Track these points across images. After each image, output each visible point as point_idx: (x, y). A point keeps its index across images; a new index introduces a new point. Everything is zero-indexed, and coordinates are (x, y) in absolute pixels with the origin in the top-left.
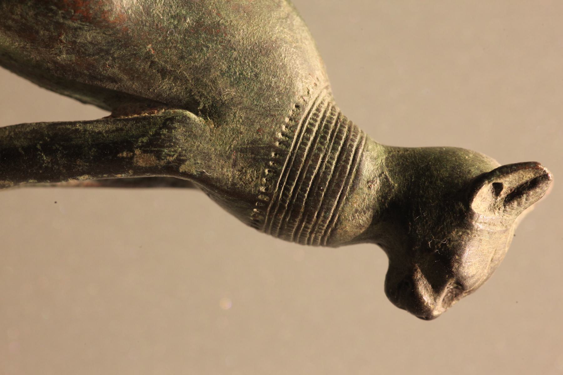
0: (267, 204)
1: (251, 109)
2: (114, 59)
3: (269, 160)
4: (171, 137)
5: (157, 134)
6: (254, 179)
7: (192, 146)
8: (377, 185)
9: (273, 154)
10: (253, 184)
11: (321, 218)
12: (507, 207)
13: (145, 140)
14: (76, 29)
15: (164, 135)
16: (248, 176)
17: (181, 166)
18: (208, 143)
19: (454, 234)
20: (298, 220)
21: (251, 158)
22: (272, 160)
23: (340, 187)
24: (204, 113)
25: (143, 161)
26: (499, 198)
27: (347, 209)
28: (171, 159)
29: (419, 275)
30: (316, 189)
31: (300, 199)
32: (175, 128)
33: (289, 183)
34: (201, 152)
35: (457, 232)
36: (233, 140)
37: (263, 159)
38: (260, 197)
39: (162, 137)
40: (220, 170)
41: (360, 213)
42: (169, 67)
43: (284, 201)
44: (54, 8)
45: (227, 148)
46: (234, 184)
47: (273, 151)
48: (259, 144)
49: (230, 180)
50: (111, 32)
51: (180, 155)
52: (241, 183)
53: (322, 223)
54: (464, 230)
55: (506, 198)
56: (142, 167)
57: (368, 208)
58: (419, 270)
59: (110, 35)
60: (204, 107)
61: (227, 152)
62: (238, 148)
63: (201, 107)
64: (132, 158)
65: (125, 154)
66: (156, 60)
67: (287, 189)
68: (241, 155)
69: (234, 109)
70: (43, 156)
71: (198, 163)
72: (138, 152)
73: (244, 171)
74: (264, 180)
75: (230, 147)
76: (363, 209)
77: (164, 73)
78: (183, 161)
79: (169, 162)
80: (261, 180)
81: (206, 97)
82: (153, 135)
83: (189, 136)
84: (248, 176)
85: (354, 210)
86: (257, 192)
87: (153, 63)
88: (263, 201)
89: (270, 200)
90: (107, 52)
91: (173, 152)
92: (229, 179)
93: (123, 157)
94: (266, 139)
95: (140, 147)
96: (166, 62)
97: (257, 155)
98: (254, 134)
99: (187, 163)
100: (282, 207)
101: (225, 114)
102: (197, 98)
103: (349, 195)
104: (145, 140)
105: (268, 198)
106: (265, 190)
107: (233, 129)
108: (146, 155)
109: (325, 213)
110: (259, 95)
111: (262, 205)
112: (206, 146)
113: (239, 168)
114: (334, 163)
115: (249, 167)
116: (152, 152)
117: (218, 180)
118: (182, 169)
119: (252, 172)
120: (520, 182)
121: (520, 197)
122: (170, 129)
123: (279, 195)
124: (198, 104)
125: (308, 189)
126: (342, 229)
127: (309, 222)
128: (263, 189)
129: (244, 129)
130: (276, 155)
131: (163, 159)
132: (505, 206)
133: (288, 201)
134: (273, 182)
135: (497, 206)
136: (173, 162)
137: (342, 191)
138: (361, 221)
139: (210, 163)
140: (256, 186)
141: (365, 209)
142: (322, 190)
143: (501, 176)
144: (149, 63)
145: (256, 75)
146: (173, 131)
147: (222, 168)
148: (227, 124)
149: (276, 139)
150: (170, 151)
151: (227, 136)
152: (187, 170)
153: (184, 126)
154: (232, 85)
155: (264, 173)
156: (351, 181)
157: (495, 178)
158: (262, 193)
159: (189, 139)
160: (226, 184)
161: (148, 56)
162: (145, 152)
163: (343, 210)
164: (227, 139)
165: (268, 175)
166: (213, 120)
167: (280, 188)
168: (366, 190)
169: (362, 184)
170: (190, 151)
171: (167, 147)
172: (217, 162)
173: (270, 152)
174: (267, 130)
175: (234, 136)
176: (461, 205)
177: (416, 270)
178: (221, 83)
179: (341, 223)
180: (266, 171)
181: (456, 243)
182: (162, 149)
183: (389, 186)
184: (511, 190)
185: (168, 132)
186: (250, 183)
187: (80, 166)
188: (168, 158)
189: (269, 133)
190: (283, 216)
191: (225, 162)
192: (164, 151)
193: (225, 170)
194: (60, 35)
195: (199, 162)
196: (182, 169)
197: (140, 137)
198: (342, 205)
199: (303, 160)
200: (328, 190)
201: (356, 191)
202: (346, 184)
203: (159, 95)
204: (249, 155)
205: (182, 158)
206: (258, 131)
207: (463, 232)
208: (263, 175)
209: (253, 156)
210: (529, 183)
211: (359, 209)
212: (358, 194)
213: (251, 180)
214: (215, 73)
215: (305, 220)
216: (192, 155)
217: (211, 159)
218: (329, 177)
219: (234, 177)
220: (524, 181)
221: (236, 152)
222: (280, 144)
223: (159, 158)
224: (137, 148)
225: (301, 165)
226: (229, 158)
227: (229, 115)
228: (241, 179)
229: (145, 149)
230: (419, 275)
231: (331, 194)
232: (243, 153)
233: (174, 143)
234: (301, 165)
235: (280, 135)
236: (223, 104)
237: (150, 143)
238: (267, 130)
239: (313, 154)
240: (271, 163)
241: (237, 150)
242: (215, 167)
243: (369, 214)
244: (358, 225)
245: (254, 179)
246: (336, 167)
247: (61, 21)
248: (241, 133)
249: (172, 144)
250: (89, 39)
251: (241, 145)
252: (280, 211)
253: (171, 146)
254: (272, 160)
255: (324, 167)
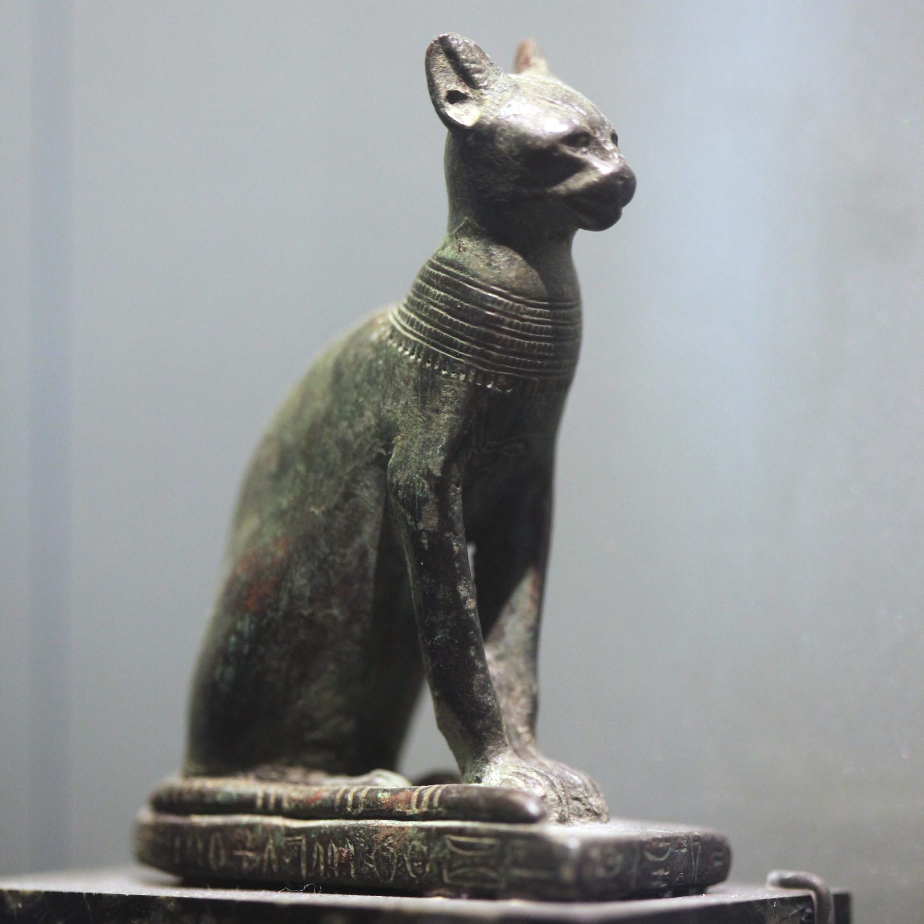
0: (478, 372)
1: (386, 391)
2: (332, 553)
3: (433, 369)
4: (405, 486)
5: (403, 503)
6: (452, 387)
7: (415, 462)
8: (465, 241)
9: (428, 365)
10: (457, 389)
11: (495, 306)
12: (481, 85)
13: (409, 517)
14: (291, 597)
15: (403, 494)
16: (449, 394)
17: (434, 474)
18: (413, 443)
19: (502, 147)
20: (498, 335)
21: (431, 391)
22: (433, 366)
23: (460, 285)
24: (389, 447)
25: (431, 519)
26: (471, 95)
27: (485, 275)
28: (426, 486)
29: (561, 188)
30: (461, 313)
31: (471, 332)
32: (397, 482)
33: (455, 345)
34: (421, 451)
35: (500, 143)
36: (413, 413)
37: (433, 377)
38: (470, 380)
39: (405, 496)
40: (441, 428)
41: (492, 260)
42: (341, 489)
43: (474, 352)
44: (265, 622)
45: (420, 419)
46: (457, 412)
47: (425, 365)
48: (418, 382)
49: (452, 415)
50: (296, 556)
51: (422, 475)
52: (456, 403)
53: (502, 306)
54: (497, 135)
55: (470, 87)
56: (439, 521)
57: (487, 251)
58: (555, 188)
59: (299, 557)
60: (383, 447)
61: (423, 420)
62: (421, 407)
63: (383, 451)
64: (428, 533)
65: (425, 541)
66: (332, 504)
67: (461, 348)
68: (428, 404)
69: (384, 412)
70: (438, 639)
71: (432, 454)
72: (421, 526)
73: (444, 400)
74: (453, 375)
75: (419, 416)
76: (487, 257)
77: (348, 495)
78: (429, 471)
79: (430, 489)
80: (453, 379)
81: (373, 446)
82: (404, 507)
83: (406, 464)
84: (449, 394)
85: (486, 268)
86: (466, 384)
87: (336, 507)
88: (476, 377)
89: (474, 367)
90: (324, 561)
91: (419, 484)
92: (452, 418)
93: (429, 543)
94: (414, 374)
95: (416, 522)
96: (335, 492)
97: (428, 383)
98: (409, 387)
99: (431, 467)
100: (481, 354)
101: (388, 423)
102: (374, 456)
103: (469, 274)
104: (409, 517)
105: (471, 371)
106: (463, 374)
107: (403, 413)
108: (423, 516)
109: (487, 301)
110: (372, 382)
111: (480, 377)
112: (416, 444)
113: (441, 405)
114: (438, 292)
115: (440, 393)
116: (420, 509)
117: (451, 431)
118: (437, 473)
119: (445, 390)
120: (451, 70)
121: (468, 70)
122: (398, 487)
123: (468, 358)
124: (380, 455)
125: (461, 322)
126: (512, 282)
127: (502, 322)
128: (462, 377)
129: (403, 400)
130: (429, 362)
131: (427, 496)
132: (481, 87)
133: (474, 346)
134: (455, 364)
135: (478, 96)
136: (430, 484)
137: (464, 282)
138: (503, 259)
139: (433, 440)
140: (459, 385)
141: (488, 255)
142: (462, 305)
143: (436, 92)
144: (337, 513)
145: (357, 386)
146: (400, 484)
147: (439, 425)
148: (398, 421)
149: (415, 362)
150: (419, 487)
151: (408, 420)
152: (439, 468)
153: (396, 471)
154: (362, 415)
155: (446, 376)
156: (455, 271)
157: (438, 100)
158: (466, 378)
159: (408, 466)
160: (457, 420)
161: (328, 513)
162: (420, 517)
163: (486, 281)
164: (411, 420)
165: (448, 371)
166: (394, 437)
167: (461, 356)
168: (467, 254)
169: (461, 258)
170: (420, 463)
171: (414, 491)
172: (433, 432)
173: (426, 369)
174: (406, 373)
175: (409, 412)
176: (470, 139)
177: (556, 192)
178: (359, 428)
179: (504, 283)
180: (444, 373)
181: (513, 145)
182: (417, 497)
183: (467, 225)
184: (461, 81)
185: (401, 490)
186: (456, 392)
187: (445, 595)
188: (425, 490)
189: (409, 371)
190: (494, 353)
191: (434, 421)
192: (419, 495)
193: (442, 422)
194: (301, 616)
195: (430, 453)
196: (437, 473)
197: (407, 523)
198: (479, 282)
199: (434, 329)
200: (462, 299)
201: (466, 266)
202: (457, 276)
203: (377, 501)
204: (428, 394)
205: (426, 473)
206: (407, 383)
207: (501, 135)
208: (447, 376)
209: (429, 389)
210: (452, 60)
211: (487, 261)
212: (469, 263)
213: (453, 391)
214: (350, 436)
215: (498, 326)
216: (424, 461)
217: (429, 438)
218: (451, 297)
219: (449, 412)
220: (449, 66)
221: (425, 409)
222: (420, 358)
223: (426, 500)
224: (417, 526)
225: (439, 331)
226: (429, 418)
227: (389, 418)
228: (452, 403)
229: (417, 517)
230: (561, 188)
231: (465, 295)
232: (425, 401)
233: (411, 483)
234: (439, 331)
235: (413, 357)
236: (378, 425)
237: (411, 510)
238: (406, 373)
239: (429, 317)
240: (436, 367)
241: (423, 408)
242: (438, 434)
243: (495, 250)
244: (508, 263)
245: (452, 387)
246: (442, 291)
247: (280, 614)
248: (407, 403)
249: (412, 484)
250: (304, 581)
251: (418, 404)
252: (488, 357)
253: (414, 487)
254: (433, 366)
255: (441, 304)
